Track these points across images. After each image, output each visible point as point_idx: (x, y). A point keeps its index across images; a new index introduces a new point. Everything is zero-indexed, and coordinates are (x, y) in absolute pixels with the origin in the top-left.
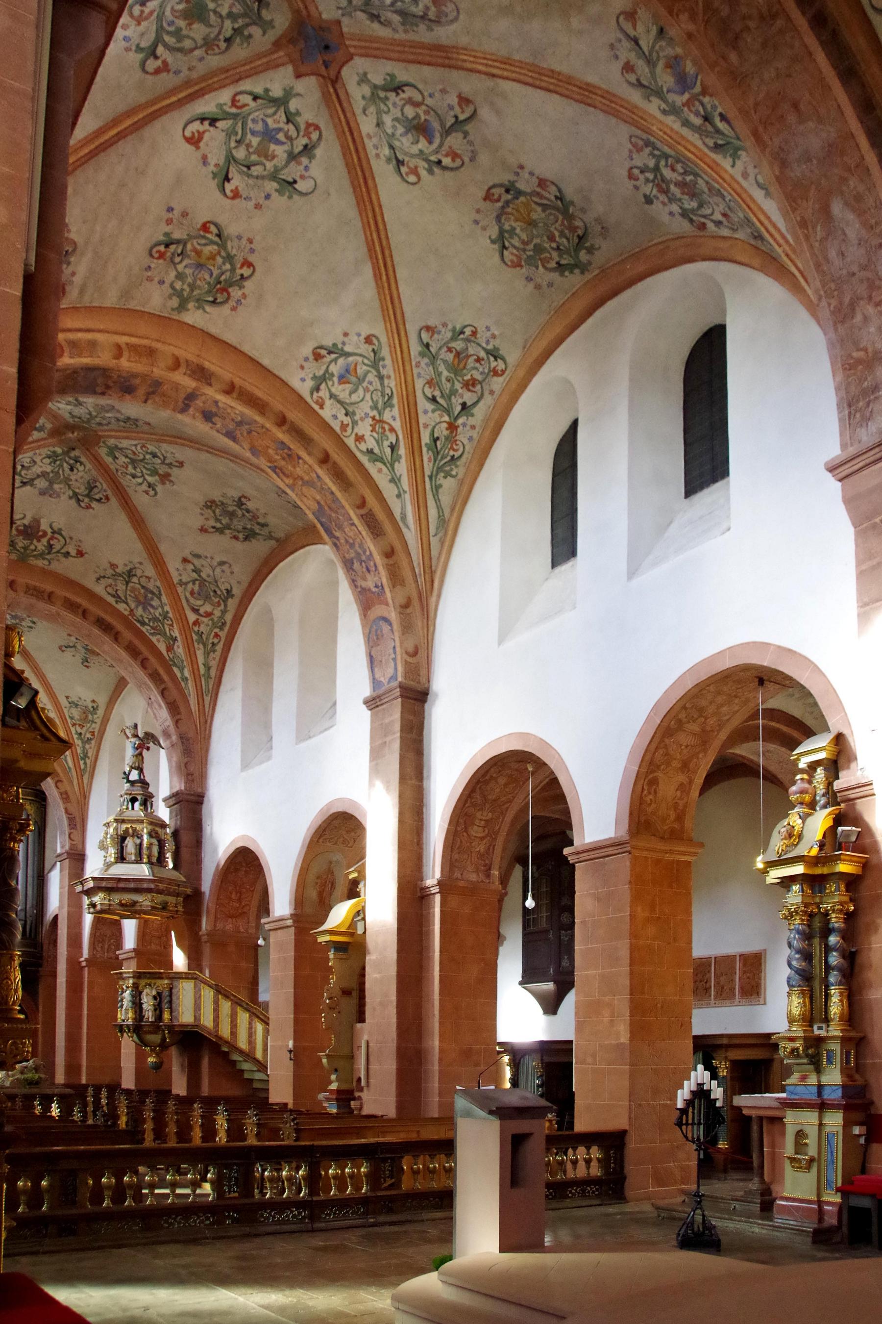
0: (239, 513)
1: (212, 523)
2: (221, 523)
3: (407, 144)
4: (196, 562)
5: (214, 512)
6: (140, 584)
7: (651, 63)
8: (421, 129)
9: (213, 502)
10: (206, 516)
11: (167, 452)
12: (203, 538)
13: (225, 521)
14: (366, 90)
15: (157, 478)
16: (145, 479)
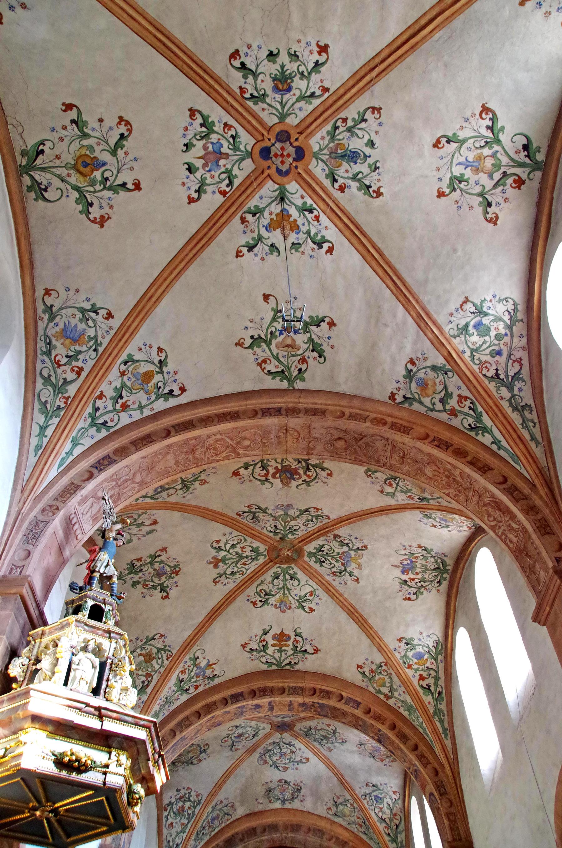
0: (156, 580)
1: (163, 558)
2: (157, 562)
3: (240, 731)
4: (146, 529)
5: (169, 566)
6: (173, 488)
7: (220, 810)
8: (240, 736)
9: (177, 573)
10: (171, 560)
11: (229, 582)
12: (159, 545)
13: (157, 566)
14: (261, 728)
15: (220, 558)
16: (229, 552)
